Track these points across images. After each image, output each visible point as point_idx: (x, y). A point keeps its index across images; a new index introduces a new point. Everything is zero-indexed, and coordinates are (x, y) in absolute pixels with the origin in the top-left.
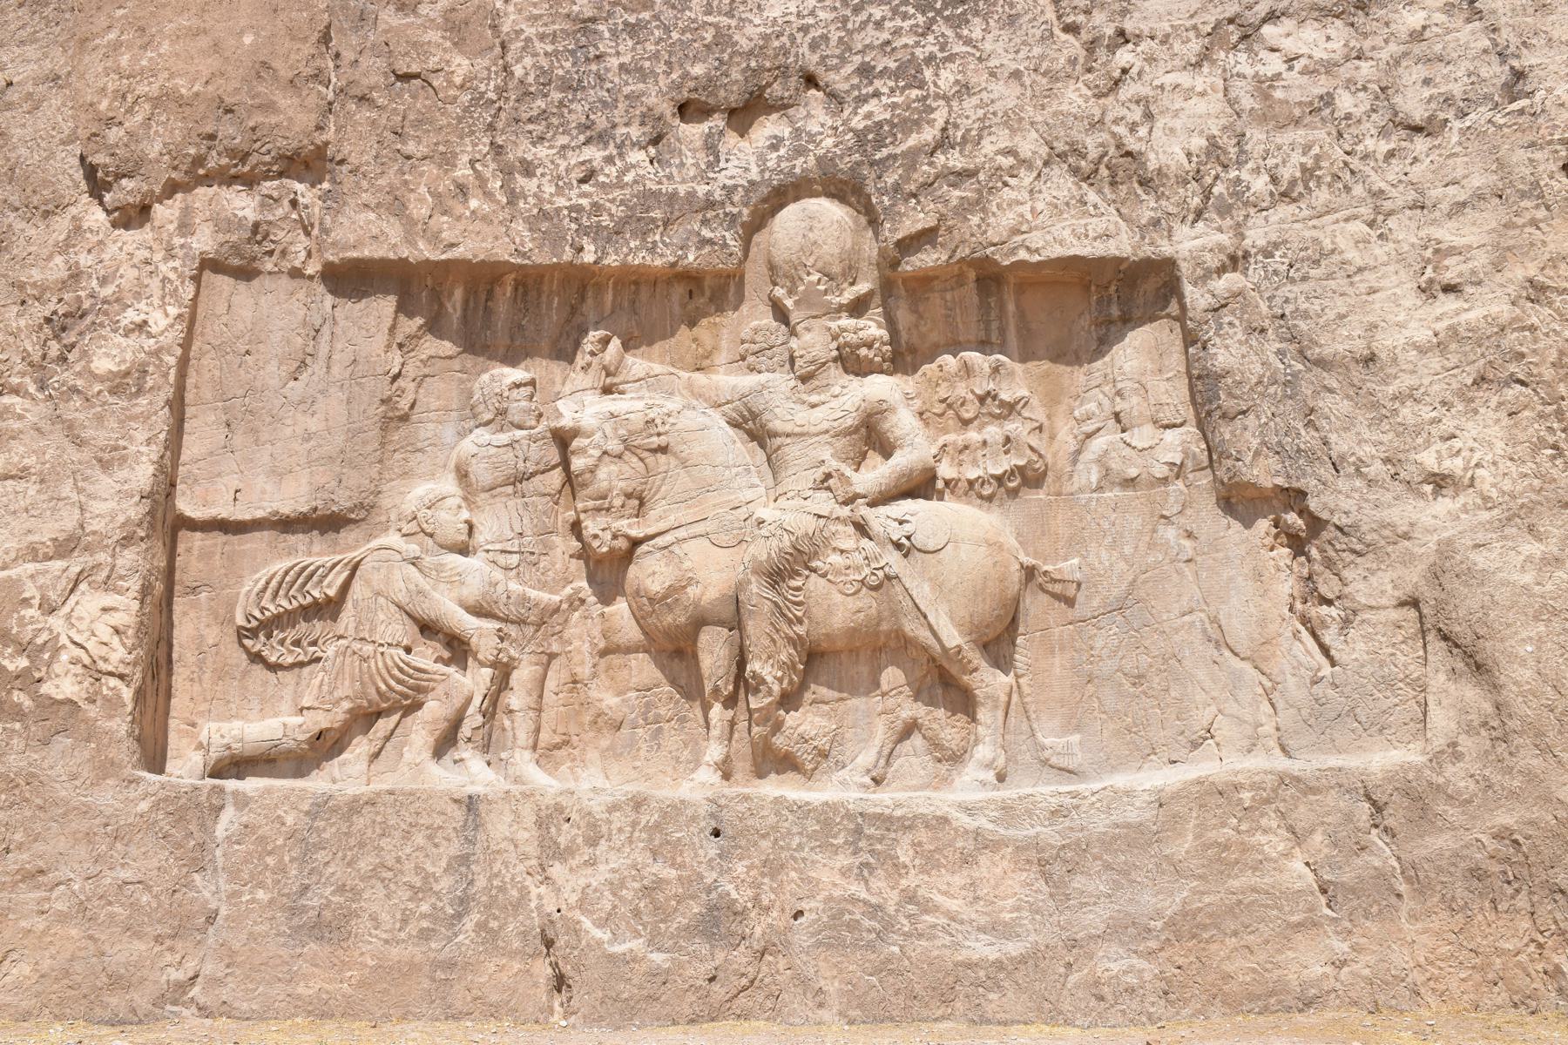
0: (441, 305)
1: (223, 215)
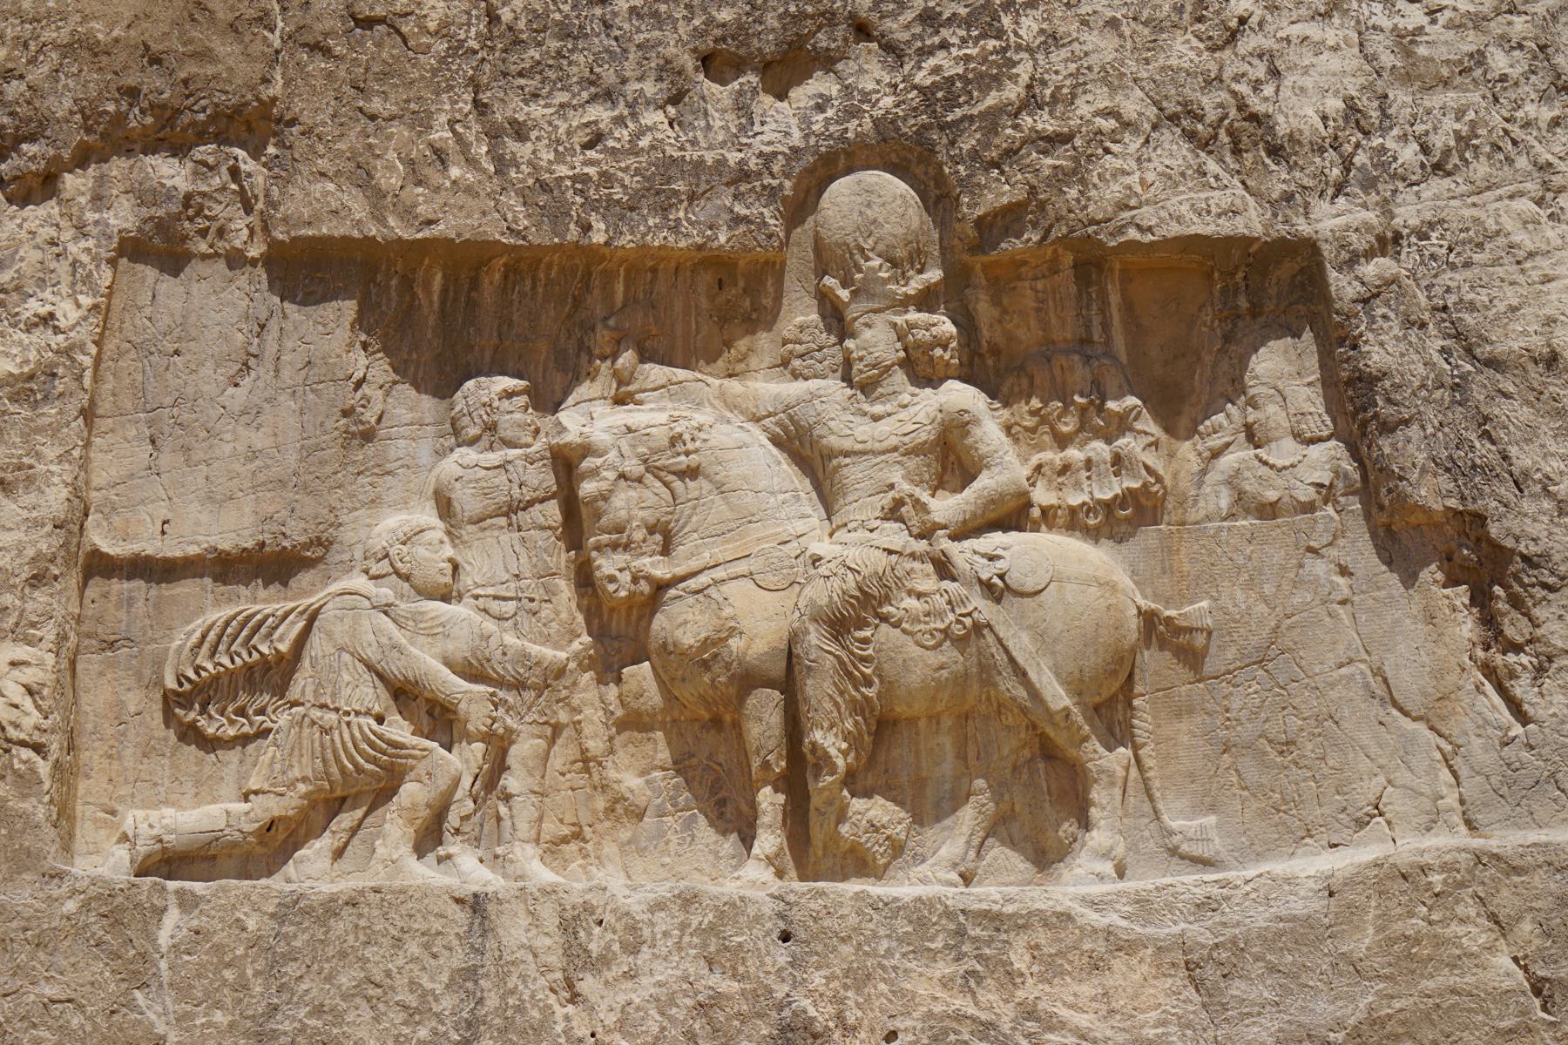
0: (414, 296)
1: (147, 185)
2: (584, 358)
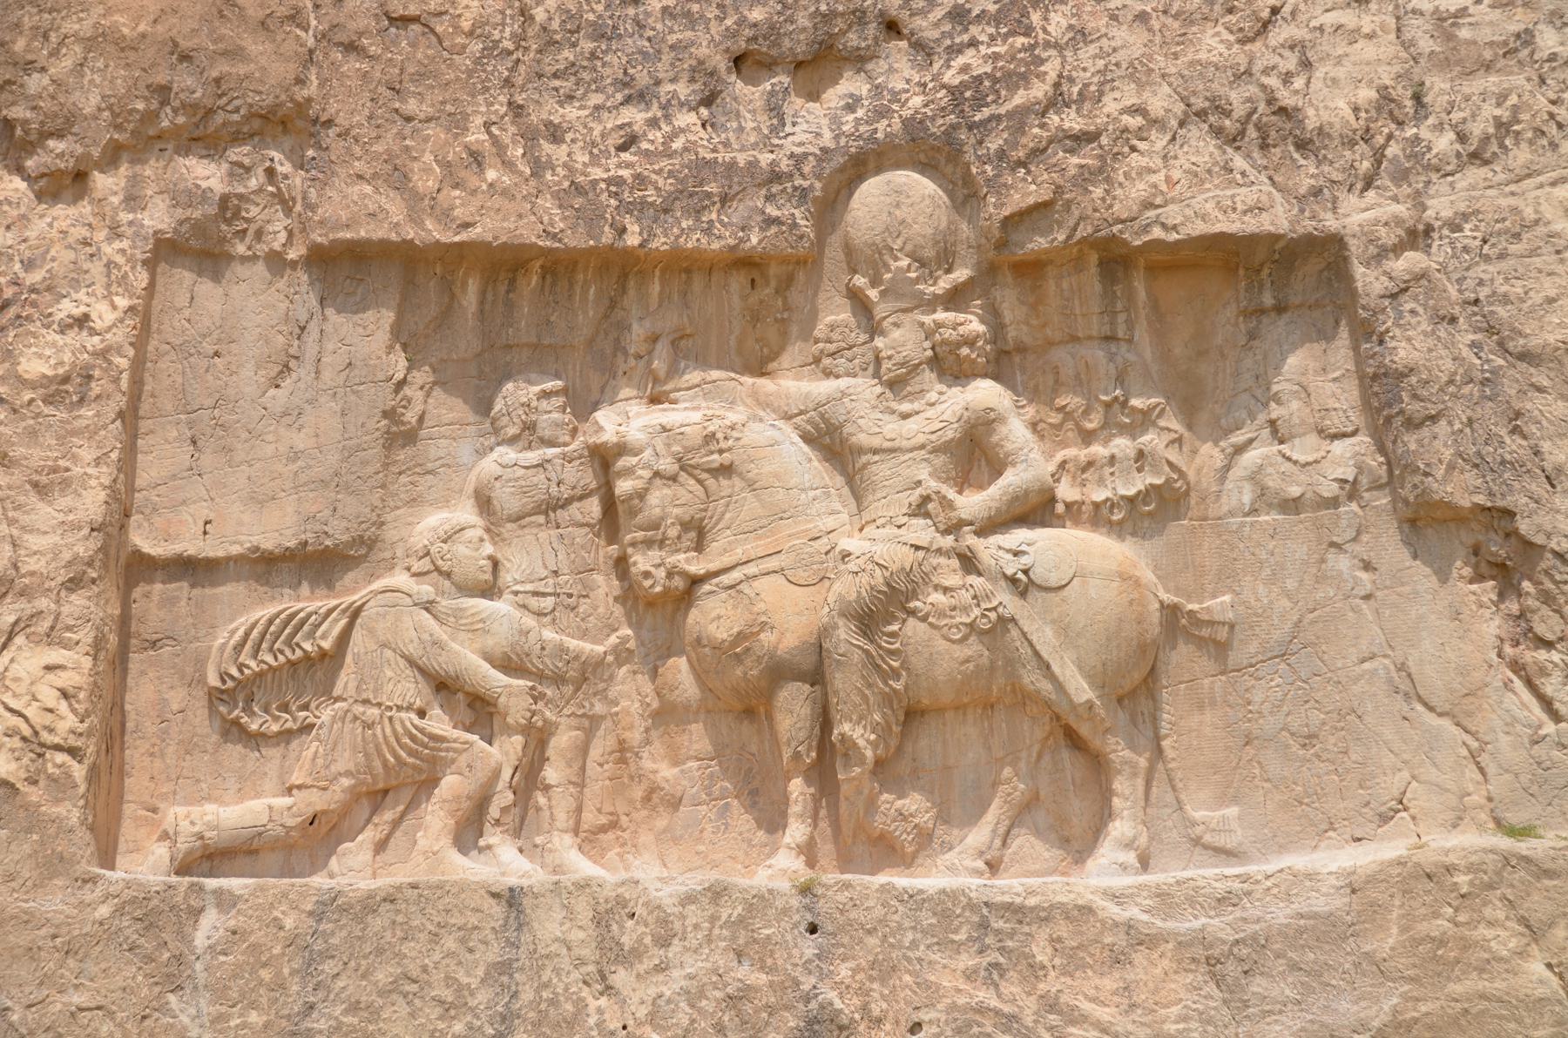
0: (453, 296)
1: (181, 186)
2: (620, 359)
